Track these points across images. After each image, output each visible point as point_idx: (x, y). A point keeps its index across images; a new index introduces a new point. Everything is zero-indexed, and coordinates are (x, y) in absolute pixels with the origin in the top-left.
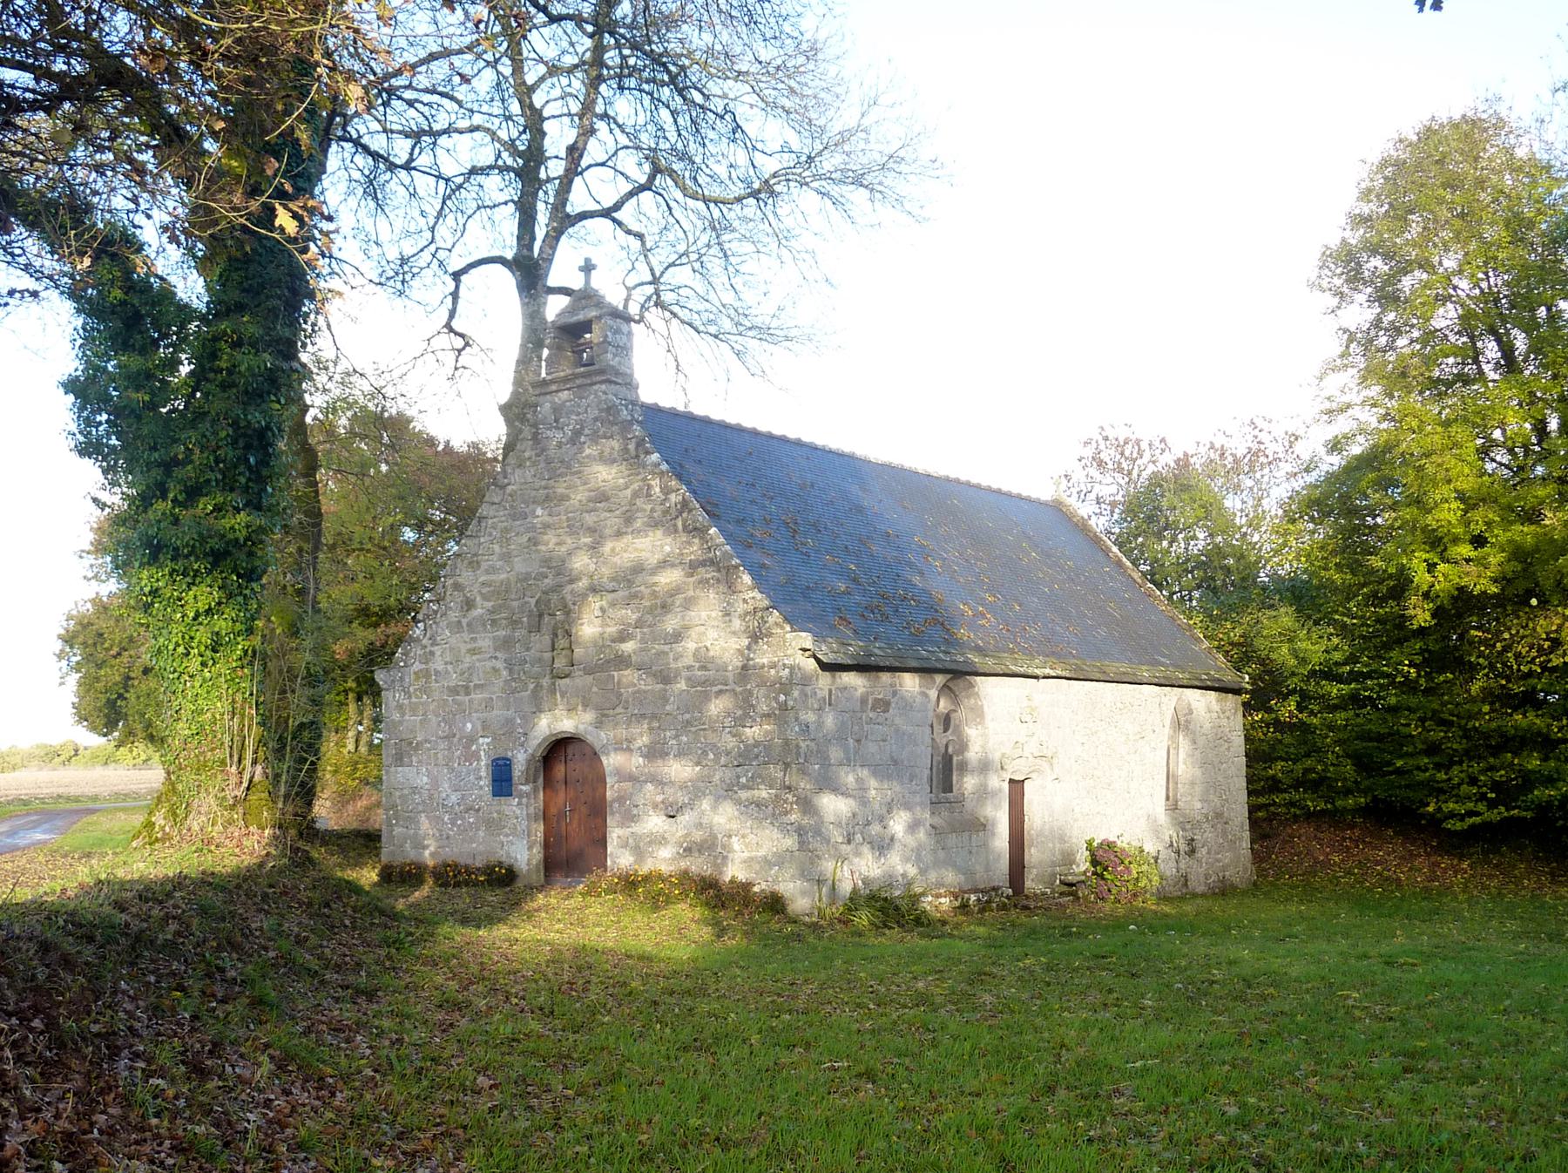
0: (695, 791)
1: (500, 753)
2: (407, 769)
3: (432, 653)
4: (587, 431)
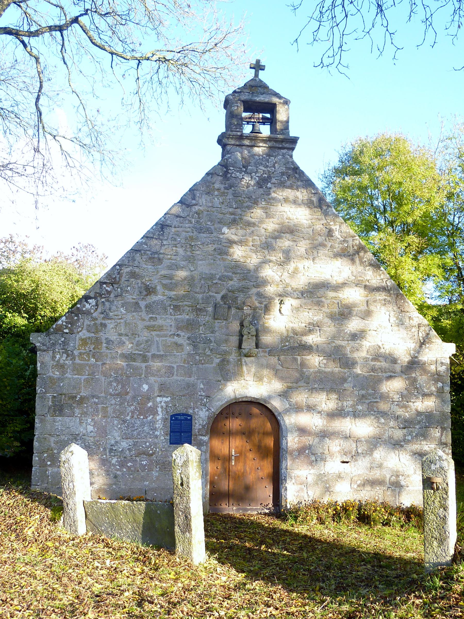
0: (374, 443)
1: (181, 409)
2: (67, 419)
3: (105, 326)
4: (274, 180)
